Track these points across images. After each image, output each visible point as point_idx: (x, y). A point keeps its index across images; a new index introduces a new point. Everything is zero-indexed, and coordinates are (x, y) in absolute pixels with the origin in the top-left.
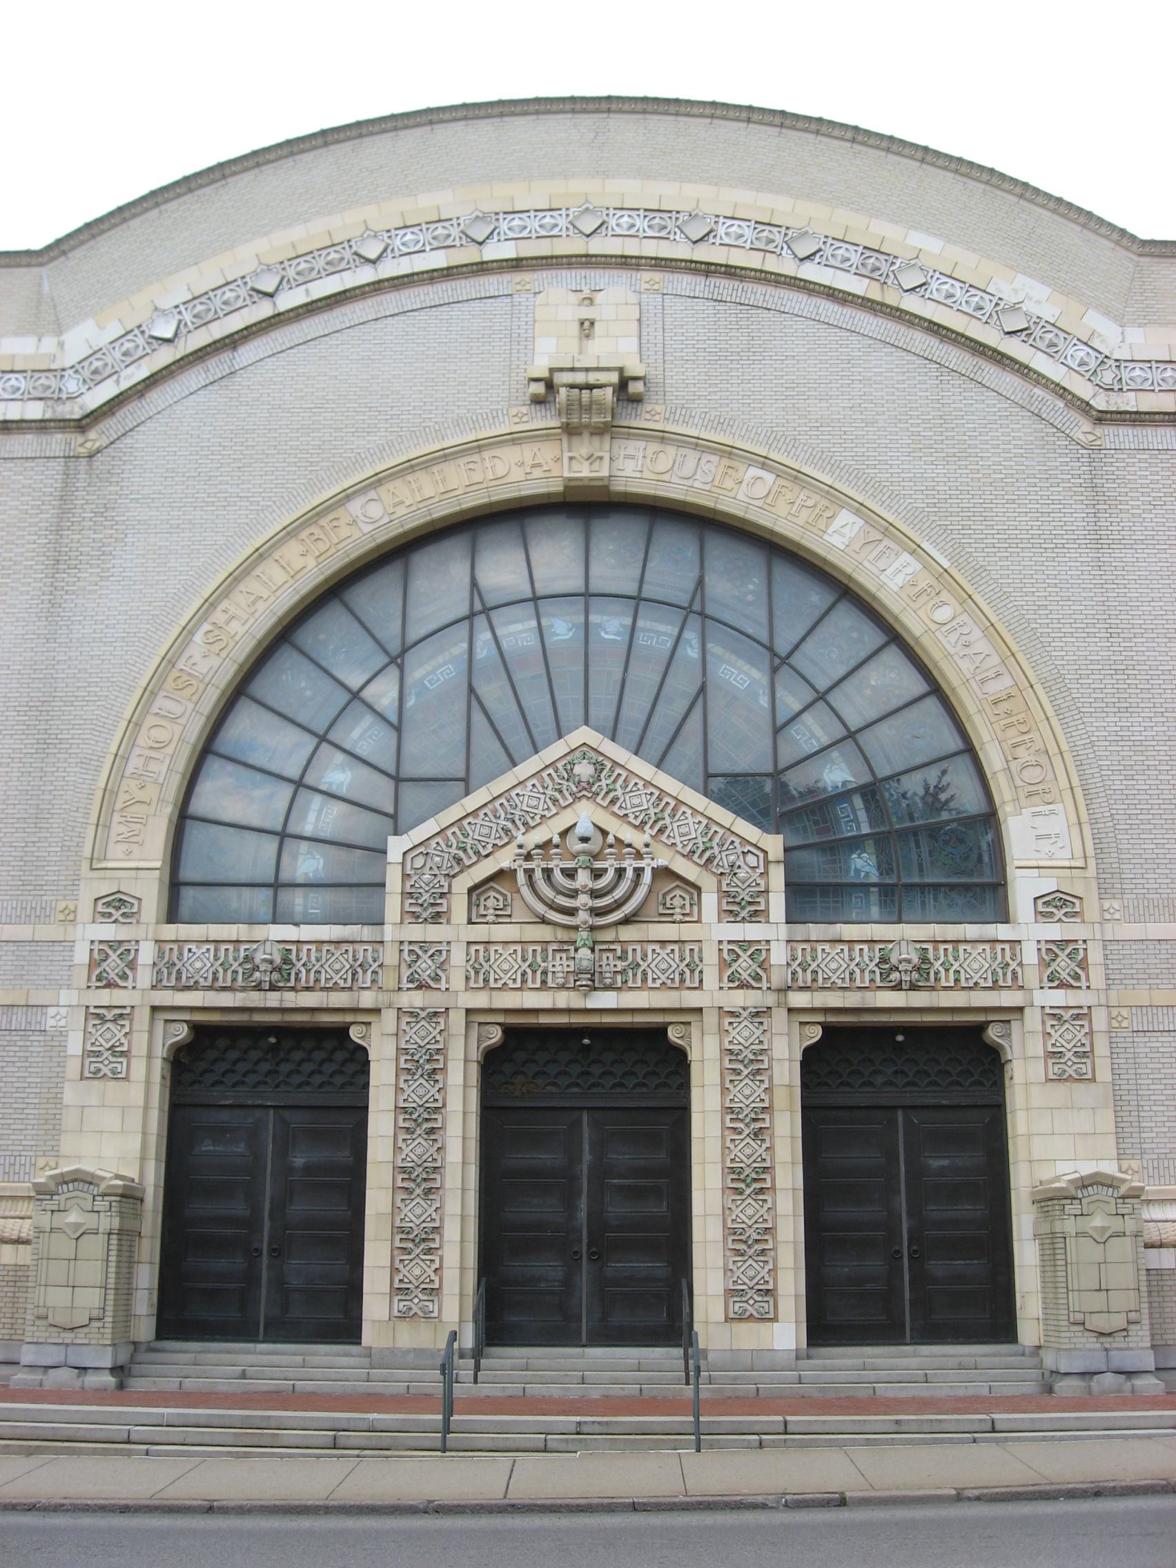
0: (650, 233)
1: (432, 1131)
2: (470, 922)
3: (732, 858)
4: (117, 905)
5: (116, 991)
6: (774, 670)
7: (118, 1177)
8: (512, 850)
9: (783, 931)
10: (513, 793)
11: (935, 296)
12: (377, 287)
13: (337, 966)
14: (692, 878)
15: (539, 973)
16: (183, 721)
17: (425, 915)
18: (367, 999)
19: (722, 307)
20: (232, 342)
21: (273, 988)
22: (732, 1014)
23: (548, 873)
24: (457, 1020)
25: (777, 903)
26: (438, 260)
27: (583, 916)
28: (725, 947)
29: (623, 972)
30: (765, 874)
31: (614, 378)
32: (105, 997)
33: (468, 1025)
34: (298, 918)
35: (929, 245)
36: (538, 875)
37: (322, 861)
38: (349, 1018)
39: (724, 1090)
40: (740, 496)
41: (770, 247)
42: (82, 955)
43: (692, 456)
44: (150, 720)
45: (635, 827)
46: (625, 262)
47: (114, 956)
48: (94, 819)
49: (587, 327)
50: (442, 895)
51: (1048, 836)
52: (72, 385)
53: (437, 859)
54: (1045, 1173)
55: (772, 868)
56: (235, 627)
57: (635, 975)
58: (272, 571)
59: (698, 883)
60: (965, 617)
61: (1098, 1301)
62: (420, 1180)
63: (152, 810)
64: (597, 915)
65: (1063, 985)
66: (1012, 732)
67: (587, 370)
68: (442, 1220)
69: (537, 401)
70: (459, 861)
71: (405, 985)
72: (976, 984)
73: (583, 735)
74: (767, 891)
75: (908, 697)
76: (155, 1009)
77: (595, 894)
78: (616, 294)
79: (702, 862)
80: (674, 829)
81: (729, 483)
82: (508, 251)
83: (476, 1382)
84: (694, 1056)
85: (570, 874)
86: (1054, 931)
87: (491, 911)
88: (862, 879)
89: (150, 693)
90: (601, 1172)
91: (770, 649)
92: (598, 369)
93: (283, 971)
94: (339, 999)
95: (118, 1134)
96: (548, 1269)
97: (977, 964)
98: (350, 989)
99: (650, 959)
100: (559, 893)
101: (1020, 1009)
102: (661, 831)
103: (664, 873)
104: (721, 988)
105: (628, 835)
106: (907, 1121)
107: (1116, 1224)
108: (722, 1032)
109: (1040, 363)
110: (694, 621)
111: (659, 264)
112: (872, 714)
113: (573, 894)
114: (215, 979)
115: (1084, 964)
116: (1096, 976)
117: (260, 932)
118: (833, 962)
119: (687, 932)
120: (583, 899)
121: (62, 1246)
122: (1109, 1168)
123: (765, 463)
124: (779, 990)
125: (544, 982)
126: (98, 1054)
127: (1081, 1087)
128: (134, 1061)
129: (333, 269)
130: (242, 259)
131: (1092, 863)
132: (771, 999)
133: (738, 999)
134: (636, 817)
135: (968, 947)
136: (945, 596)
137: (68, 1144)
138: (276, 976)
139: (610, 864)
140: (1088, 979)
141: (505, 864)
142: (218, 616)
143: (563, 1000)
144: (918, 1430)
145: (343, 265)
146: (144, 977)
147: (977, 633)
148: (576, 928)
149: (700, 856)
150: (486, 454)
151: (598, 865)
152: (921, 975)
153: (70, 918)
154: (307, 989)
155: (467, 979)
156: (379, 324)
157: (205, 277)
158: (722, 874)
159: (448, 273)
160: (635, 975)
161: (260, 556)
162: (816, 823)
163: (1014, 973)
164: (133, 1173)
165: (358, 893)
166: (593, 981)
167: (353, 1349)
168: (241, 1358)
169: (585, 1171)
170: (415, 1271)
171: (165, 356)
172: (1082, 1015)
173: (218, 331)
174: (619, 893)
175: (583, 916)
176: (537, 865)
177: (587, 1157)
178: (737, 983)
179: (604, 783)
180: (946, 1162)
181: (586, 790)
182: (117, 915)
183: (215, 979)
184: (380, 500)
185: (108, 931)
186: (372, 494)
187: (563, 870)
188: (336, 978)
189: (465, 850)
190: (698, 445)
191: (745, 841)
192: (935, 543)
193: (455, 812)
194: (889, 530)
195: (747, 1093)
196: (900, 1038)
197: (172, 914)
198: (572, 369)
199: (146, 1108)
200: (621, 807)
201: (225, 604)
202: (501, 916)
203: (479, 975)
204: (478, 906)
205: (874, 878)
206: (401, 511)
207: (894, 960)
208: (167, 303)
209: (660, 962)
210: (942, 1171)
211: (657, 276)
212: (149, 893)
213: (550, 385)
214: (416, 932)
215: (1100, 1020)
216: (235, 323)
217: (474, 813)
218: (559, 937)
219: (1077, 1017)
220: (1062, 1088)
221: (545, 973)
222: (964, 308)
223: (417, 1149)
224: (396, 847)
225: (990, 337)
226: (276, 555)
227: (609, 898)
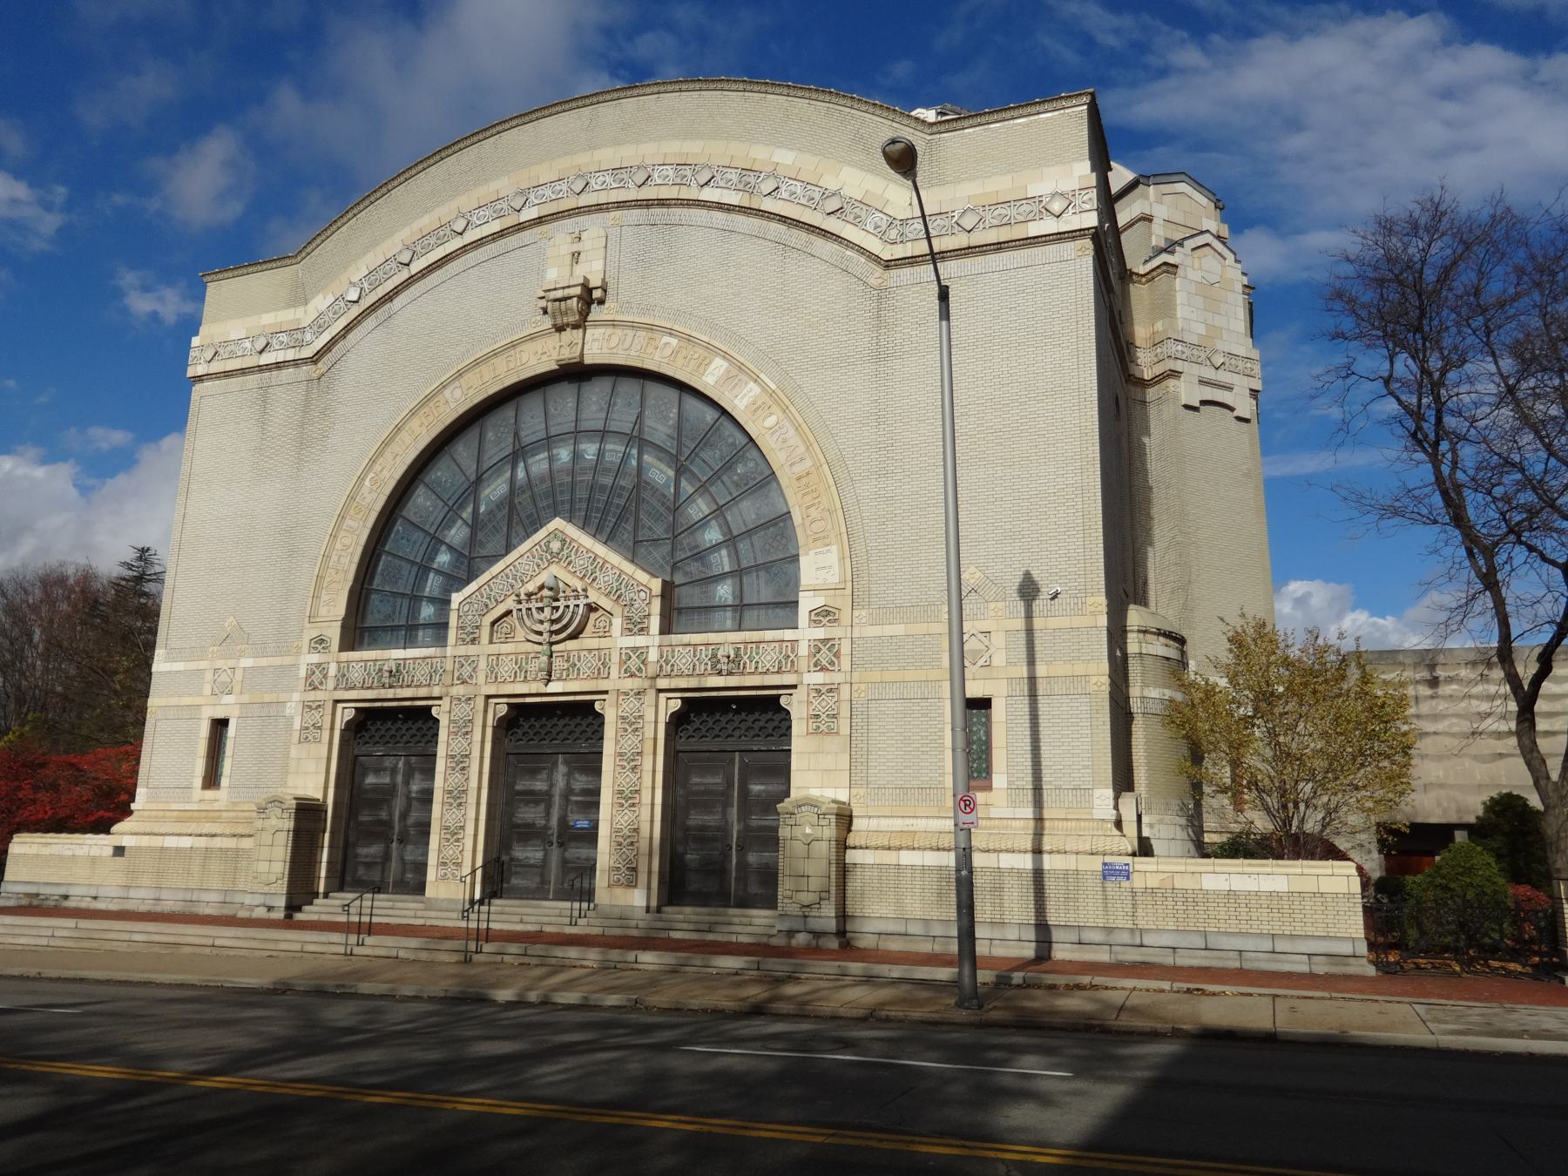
1: (463, 769)
9: (657, 640)
12: (464, 249)
18: (436, 692)
19: (655, 229)
21: (391, 687)
22: (626, 694)
26: (495, 226)
32: (312, 695)
35: (784, 157)
38: (430, 703)
42: (303, 673)
43: (630, 333)
44: (342, 533)
46: (600, 208)
58: (405, 437)
66: (806, 498)
73: (557, 523)
76: (337, 701)
77: (553, 622)
78: (594, 227)
85: (541, 609)
86: (820, 633)
89: (342, 517)
90: (568, 792)
93: (396, 675)
94: (422, 692)
95: (313, 777)
96: (530, 853)
97: (768, 658)
101: (795, 687)
106: (741, 760)
109: (849, 232)
111: (621, 205)
115: (837, 655)
116: (845, 663)
119: (604, 643)
121: (266, 838)
123: (671, 332)
127: (828, 739)
130: (393, 245)
133: (630, 684)
136: (775, 408)
137: (291, 781)
142: (377, 467)
146: (331, 683)
147: (792, 431)
152: (735, 663)
153: (298, 653)
157: (373, 259)
159: (501, 234)
161: (398, 429)
164: (320, 796)
167: (419, 898)
171: (355, 311)
173: (381, 292)
176: (524, 606)
180: (762, 787)
181: (555, 557)
186: (457, 384)
190: (633, 325)
191: (639, 584)
194: (741, 367)
195: (630, 742)
206: (471, 392)
208: (355, 279)
209: (587, 664)
210: (759, 794)
211: (618, 213)
212: (334, 633)
214: (463, 650)
215: (845, 692)
216: (389, 286)
219: (831, 690)
220: (817, 738)
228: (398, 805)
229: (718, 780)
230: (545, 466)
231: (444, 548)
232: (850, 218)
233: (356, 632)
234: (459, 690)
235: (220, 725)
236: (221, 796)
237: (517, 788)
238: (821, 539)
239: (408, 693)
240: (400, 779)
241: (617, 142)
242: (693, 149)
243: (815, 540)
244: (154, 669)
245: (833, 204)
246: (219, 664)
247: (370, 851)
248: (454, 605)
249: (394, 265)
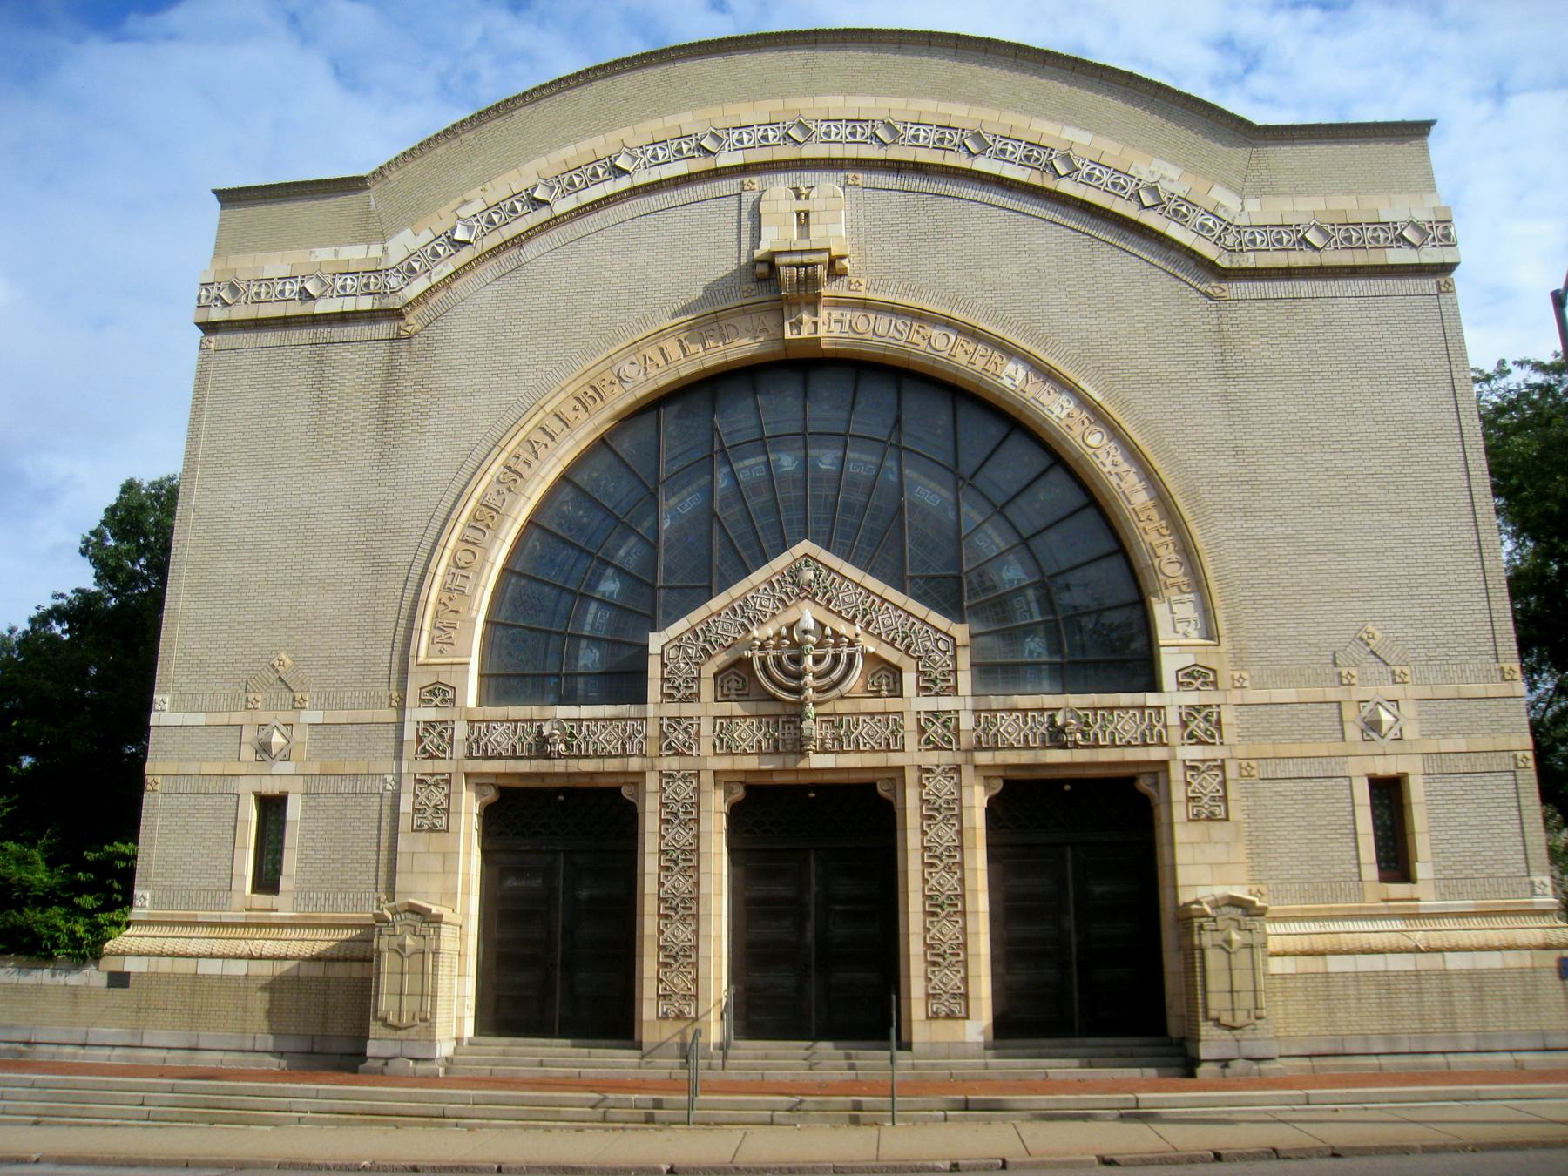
6: (957, 490)
13: (606, 738)
18: (634, 764)
20: (518, 241)
23: (778, 660)
25: (965, 680)
26: (681, 168)
28: (922, 716)
30: (954, 657)
31: (825, 257)
32: (429, 766)
36: (770, 661)
38: (621, 780)
49: (804, 219)
52: (394, 282)
55: (960, 651)
65: (1200, 742)
74: (955, 671)
76: (467, 775)
78: (826, 185)
82: (737, 159)
86: (1192, 698)
94: (612, 765)
105: (843, 628)
109: (1174, 231)
110: (891, 452)
112: (1041, 524)
114: (514, 750)
118: (1008, 726)
122: (1240, 892)
124: (967, 751)
125: (776, 748)
132: (960, 758)
133: (932, 758)
140: (1221, 736)
144: (1087, 1105)
146: (460, 750)
154: (587, 757)
162: (997, 613)
165: (625, 682)
174: (835, 675)
177: (814, 888)
181: (808, 593)
191: (938, 630)
196: (1067, 787)
198: (790, 252)
203: (723, 745)
205: (1045, 659)
214: (673, 709)
215: (1232, 771)
224: (656, 642)
231: (610, 572)
234: (670, 763)
235: (272, 808)
236: (283, 905)
239: (588, 765)
241: (847, 91)
242: (960, 113)
244: (154, 719)
246: (265, 717)
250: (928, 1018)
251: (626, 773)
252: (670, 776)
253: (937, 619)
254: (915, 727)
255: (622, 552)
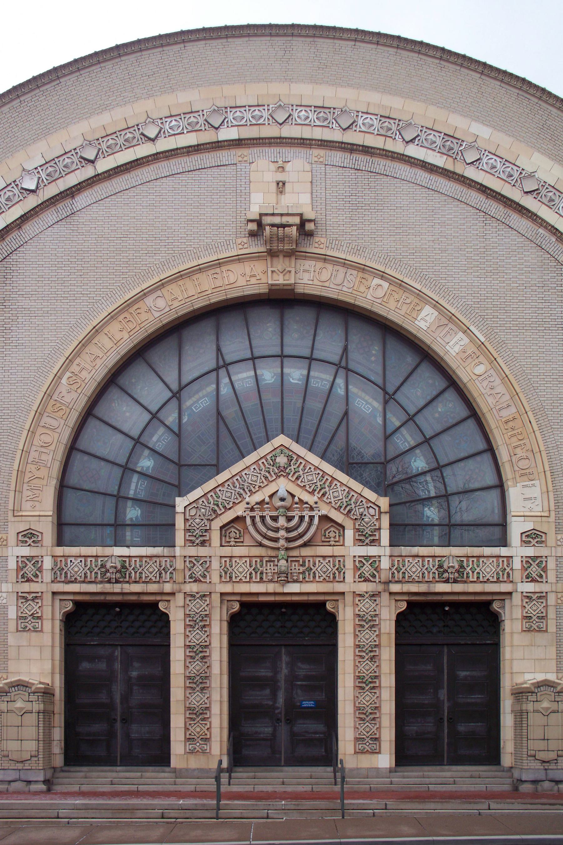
0: (318, 123)
2: (221, 546)
3: (362, 510)
4: (29, 537)
5: (32, 584)
6: (386, 402)
7: (41, 683)
8: (243, 506)
9: (388, 551)
10: (243, 473)
11: (485, 167)
12: (156, 157)
14: (340, 521)
15: (259, 573)
16: (59, 430)
17: (197, 541)
18: (168, 588)
19: (359, 174)
20: (71, 193)
21: (117, 582)
22: (360, 595)
23: (263, 518)
24: (216, 598)
26: (191, 139)
27: (282, 542)
29: (303, 573)
30: (379, 519)
31: (297, 220)
32: (26, 587)
33: (222, 602)
34: (128, 543)
36: (258, 519)
37: (139, 511)
38: (158, 598)
39: (356, 636)
40: (369, 297)
41: (389, 134)
42: (12, 564)
43: (342, 270)
44: (40, 430)
45: (309, 492)
47: (30, 565)
48: (13, 487)
49: (281, 186)
50: (206, 531)
51: (530, 499)
53: (203, 510)
54: (519, 679)
56: (84, 374)
57: (309, 574)
58: (103, 340)
59: (344, 524)
60: (492, 371)
61: (542, 745)
62: (198, 682)
63: (45, 482)
64: (289, 542)
65: (533, 581)
66: (514, 439)
67: (282, 215)
68: (210, 703)
69: (252, 234)
70: (215, 511)
71: (187, 580)
72: (488, 579)
73: (281, 440)
75: (458, 418)
76: (54, 593)
77: (288, 530)
78: (298, 164)
79: (345, 512)
80: (331, 495)
81: (362, 289)
83: (229, 784)
84: (340, 617)
85: (275, 519)
86: (530, 551)
87: (233, 539)
88: (430, 522)
89: (39, 414)
91: (384, 390)
92: (288, 215)
93: (122, 572)
95: (39, 661)
97: (489, 569)
98: (159, 582)
99: (317, 566)
100: (269, 529)
101: (510, 593)
102: (324, 495)
103: (325, 518)
104: (355, 581)
105: (306, 497)
107: (554, 706)
108: (355, 605)
109: (545, 213)
110: (342, 372)
112: (439, 428)
113: (277, 530)
114: (86, 577)
115: (545, 569)
116: (551, 576)
117: (108, 551)
118: (413, 568)
119: (338, 551)
120: (282, 533)
122: (552, 677)
123: (383, 276)
124: (385, 583)
125: (261, 578)
126: (26, 618)
128: (45, 622)
129: (129, 144)
130: (73, 135)
131: (553, 514)
132: (380, 588)
133: (363, 587)
134: (310, 487)
135: (485, 560)
136: (482, 358)
137: (12, 666)
138: (118, 575)
139: (296, 514)
140: (547, 577)
141: (240, 513)
142: (74, 368)
143: (271, 588)
145: (135, 142)
146: (47, 576)
147: (498, 381)
148: (278, 549)
149: (345, 509)
150: (224, 268)
151: (290, 514)
152: (460, 575)
154: (136, 582)
155: (221, 576)
156: (158, 183)
158: (356, 519)
160: (309, 574)
161: (96, 331)
163: (508, 574)
164: (48, 681)
165: (159, 530)
166: (288, 578)
167: (167, 769)
168: (109, 774)
169: (283, 678)
170: (196, 729)
171: (32, 202)
172: (542, 596)
175: (282, 542)
178: (363, 579)
179: (292, 467)
181: (283, 472)
182: (30, 542)
183: (86, 577)
184: (163, 296)
185: (25, 551)
186: (159, 293)
187: (271, 517)
188: (151, 576)
189: (218, 506)
190: (345, 264)
192: (477, 327)
193: (211, 484)
194: (451, 318)
195: (367, 637)
197: (60, 542)
198: (273, 215)
199: (53, 646)
200: (302, 481)
201: (78, 361)
202: (239, 543)
203: (227, 575)
204: (225, 536)
206: (176, 304)
207: (445, 566)
208: (30, 166)
209: (321, 567)
211: (322, 152)
213: (259, 223)
214: (192, 551)
215: (552, 599)
216: (72, 180)
217: (222, 484)
218: (269, 554)
219: (540, 598)
220: (529, 635)
221: (262, 573)
222: (502, 176)
223: (196, 667)
224: (181, 503)
225: (515, 195)
226: (106, 331)
227: (295, 531)
228: (118, 690)
229: (429, 667)
230: (251, 383)
232: (545, 200)
233: (65, 530)
234: (194, 588)
237: (243, 674)
238: (527, 475)
240: (117, 666)
242: (395, 104)
243: (522, 475)
245: (530, 186)
247: (98, 727)
248: (180, 508)
249: (75, 159)
250: (356, 753)
251: (162, 594)
252: (192, 596)
253: (371, 495)
254: (352, 566)
255: (155, 439)
